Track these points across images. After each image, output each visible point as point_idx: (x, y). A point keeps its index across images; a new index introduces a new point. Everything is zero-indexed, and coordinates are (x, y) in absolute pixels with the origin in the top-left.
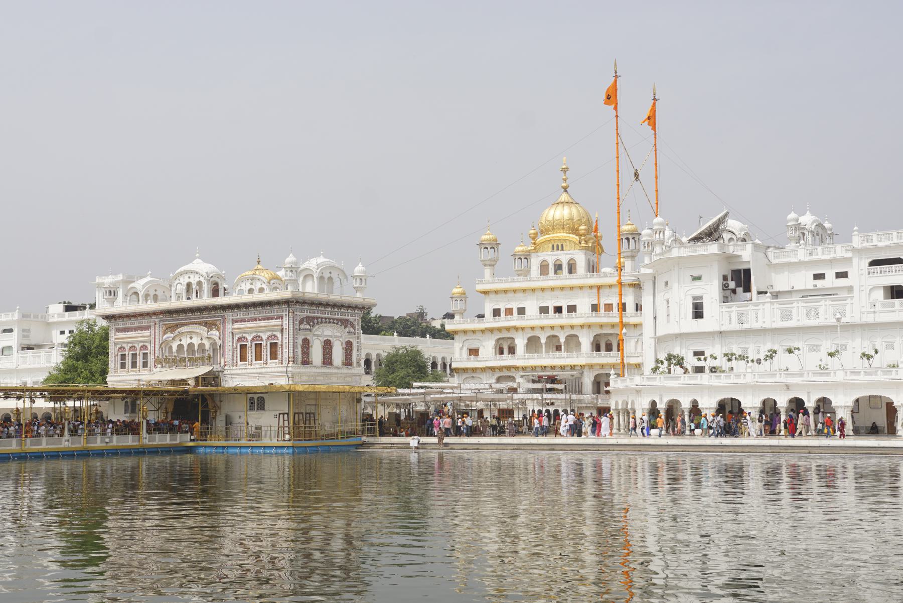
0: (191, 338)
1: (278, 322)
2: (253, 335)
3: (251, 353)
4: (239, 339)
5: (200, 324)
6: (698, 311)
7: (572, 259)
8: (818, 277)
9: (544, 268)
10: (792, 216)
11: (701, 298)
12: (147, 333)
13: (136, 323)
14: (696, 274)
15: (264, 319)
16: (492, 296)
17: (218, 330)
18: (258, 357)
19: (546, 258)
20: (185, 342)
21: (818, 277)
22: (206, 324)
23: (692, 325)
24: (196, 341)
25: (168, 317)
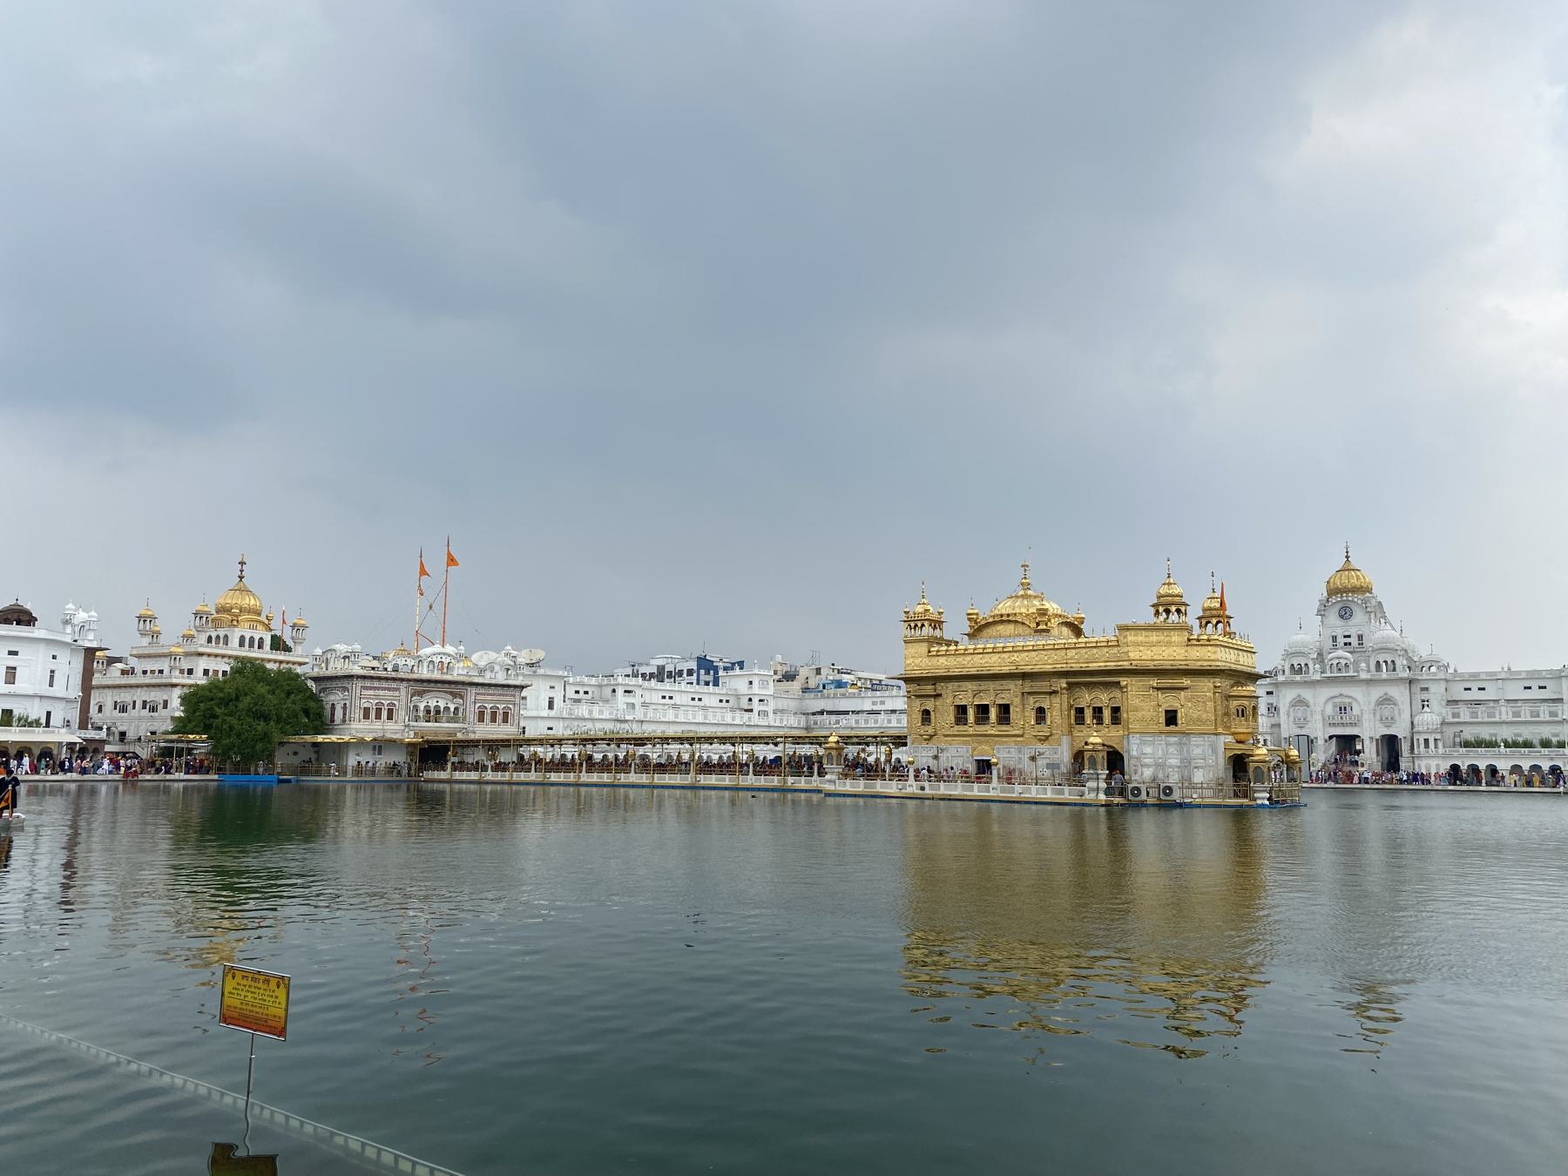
0: (437, 702)
1: (512, 699)
2: (491, 705)
3: (487, 717)
4: (479, 708)
5: (445, 692)
6: (551, 706)
7: (261, 638)
8: (577, 692)
9: (242, 639)
10: (509, 647)
11: (553, 698)
12: (397, 693)
13: (385, 684)
14: (552, 685)
15: (500, 695)
16: (205, 658)
17: (462, 698)
18: (493, 720)
19: (244, 634)
20: (432, 704)
21: (577, 692)
22: (451, 693)
23: (545, 713)
24: (442, 704)
25: (419, 684)
